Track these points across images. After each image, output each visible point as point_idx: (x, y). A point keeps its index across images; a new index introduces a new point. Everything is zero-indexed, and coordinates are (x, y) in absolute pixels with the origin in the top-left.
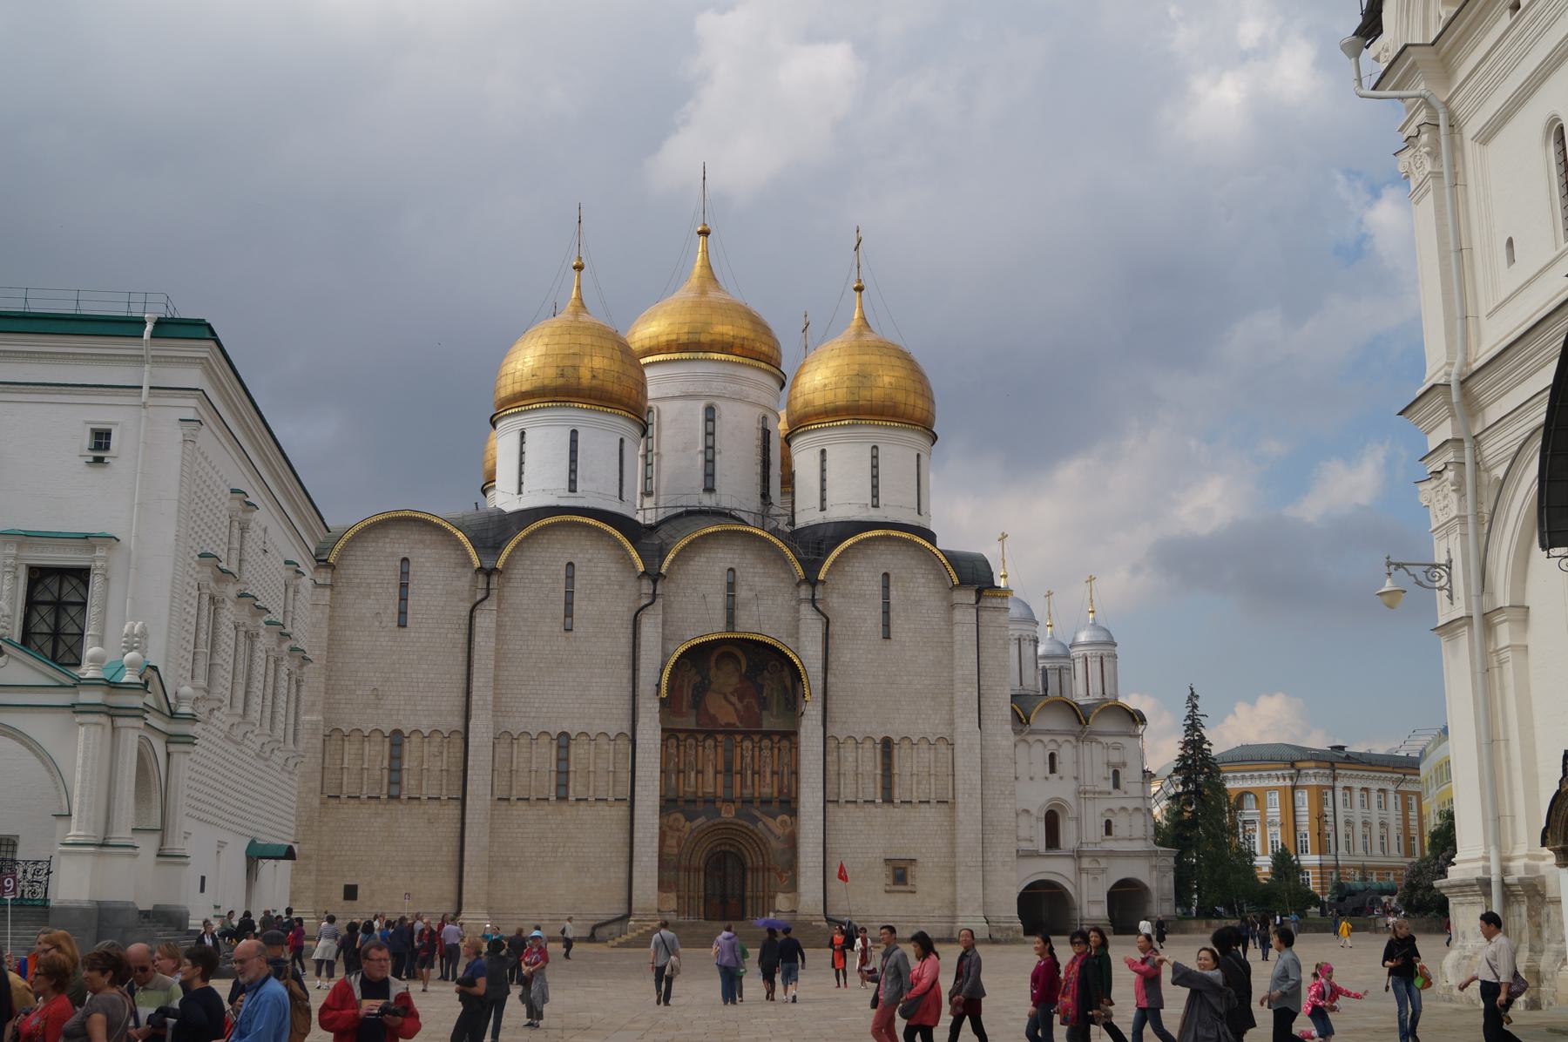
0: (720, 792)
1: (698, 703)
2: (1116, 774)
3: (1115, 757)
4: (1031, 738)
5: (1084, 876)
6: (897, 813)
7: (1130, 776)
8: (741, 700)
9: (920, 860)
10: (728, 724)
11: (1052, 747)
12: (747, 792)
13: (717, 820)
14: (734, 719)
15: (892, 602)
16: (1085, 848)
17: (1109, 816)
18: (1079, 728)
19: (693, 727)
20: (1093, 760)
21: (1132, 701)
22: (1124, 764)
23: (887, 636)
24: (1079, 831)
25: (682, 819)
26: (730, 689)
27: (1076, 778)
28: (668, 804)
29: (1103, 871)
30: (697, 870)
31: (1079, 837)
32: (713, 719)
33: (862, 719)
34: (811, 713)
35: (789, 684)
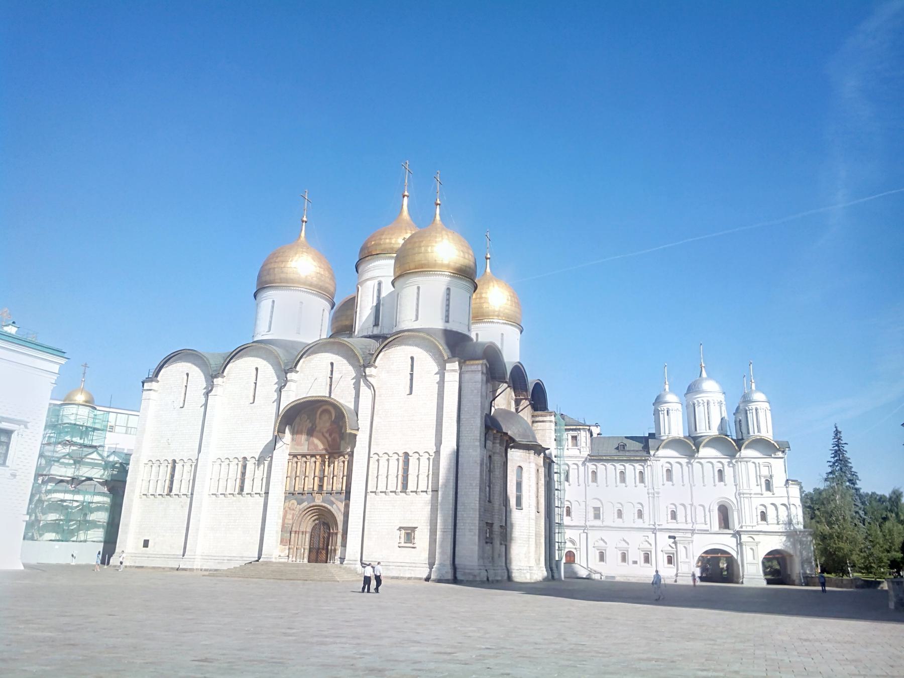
0: (316, 488)
8: (330, 435)
24: (746, 517)
26: (325, 430)
28: (290, 495)
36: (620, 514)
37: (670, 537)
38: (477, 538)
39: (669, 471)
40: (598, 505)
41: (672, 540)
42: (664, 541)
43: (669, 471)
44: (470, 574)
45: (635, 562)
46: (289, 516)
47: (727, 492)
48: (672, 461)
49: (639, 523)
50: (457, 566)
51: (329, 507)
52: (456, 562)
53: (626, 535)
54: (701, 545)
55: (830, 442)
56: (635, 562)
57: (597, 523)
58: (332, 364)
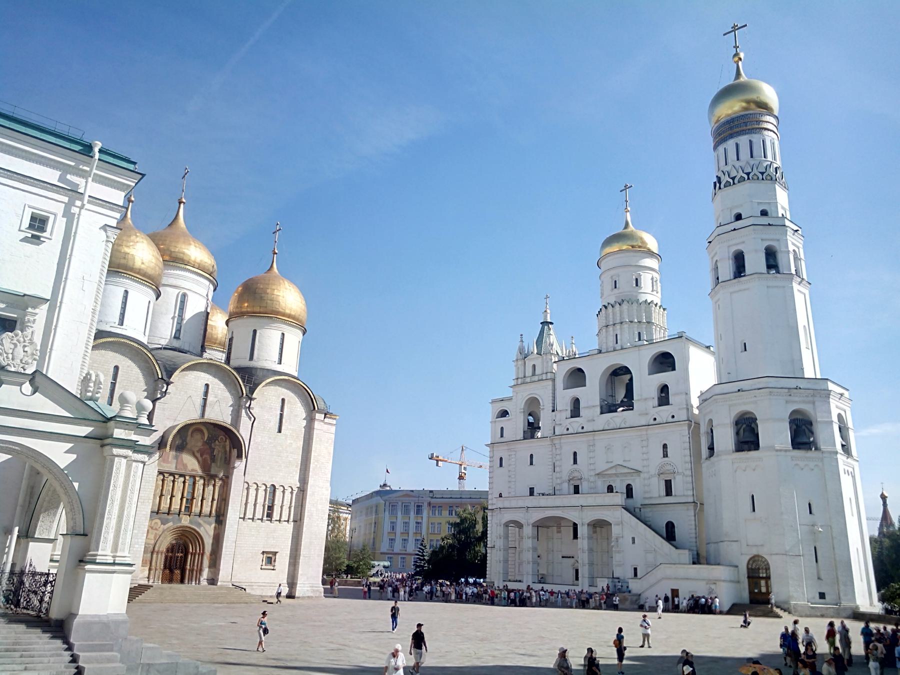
8: (201, 456)
13: (179, 525)
15: (285, 414)
19: (173, 470)
23: (280, 431)
26: (196, 449)
32: (185, 466)
34: (239, 465)
35: (228, 449)
58: (207, 385)
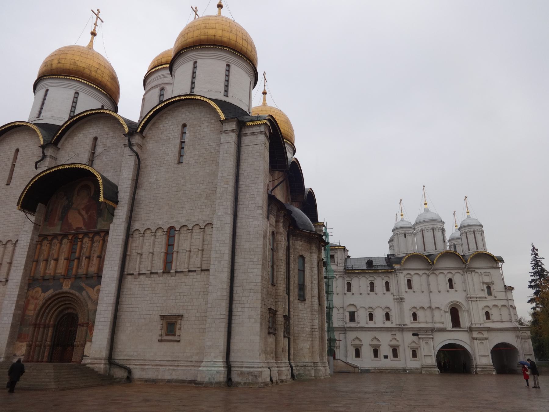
1: (64, 218)
2: (489, 288)
3: (487, 279)
4: (437, 272)
5: (475, 341)
6: (172, 280)
7: (497, 288)
8: (87, 213)
9: (186, 315)
10: (78, 228)
11: (450, 276)
12: (82, 271)
14: (81, 225)
16: (474, 326)
17: (487, 309)
18: (464, 266)
20: (474, 282)
21: (495, 254)
22: (493, 283)
25: (40, 292)
27: (465, 291)
29: (487, 338)
30: (46, 326)
31: (470, 320)
33: (155, 215)
36: (371, 317)
37: (414, 335)
38: (258, 325)
39: (409, 281)
40: (352, 309)
41: (416, 337)
42: (409, 338)
43: (409, 281)
44: (249, 373)
45: (386, 357)
46: (31, 307)
47: (457, 296)
48: (412, 272)
49: (388, 324)
50: (233, 364)
51: (77, 294)
52: (232, 359)
53: (378, 335)
54: (442, 340)
55: (530, 257)
56: (386, 357)
57: (353, 325)
